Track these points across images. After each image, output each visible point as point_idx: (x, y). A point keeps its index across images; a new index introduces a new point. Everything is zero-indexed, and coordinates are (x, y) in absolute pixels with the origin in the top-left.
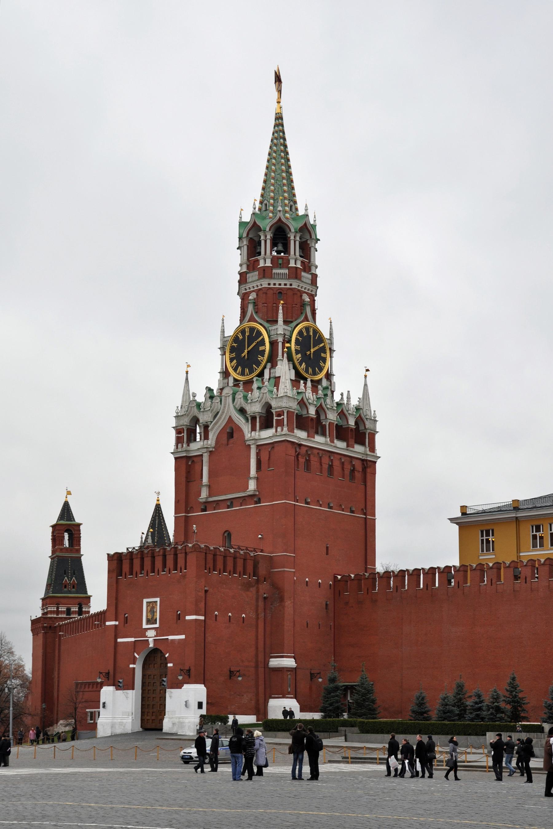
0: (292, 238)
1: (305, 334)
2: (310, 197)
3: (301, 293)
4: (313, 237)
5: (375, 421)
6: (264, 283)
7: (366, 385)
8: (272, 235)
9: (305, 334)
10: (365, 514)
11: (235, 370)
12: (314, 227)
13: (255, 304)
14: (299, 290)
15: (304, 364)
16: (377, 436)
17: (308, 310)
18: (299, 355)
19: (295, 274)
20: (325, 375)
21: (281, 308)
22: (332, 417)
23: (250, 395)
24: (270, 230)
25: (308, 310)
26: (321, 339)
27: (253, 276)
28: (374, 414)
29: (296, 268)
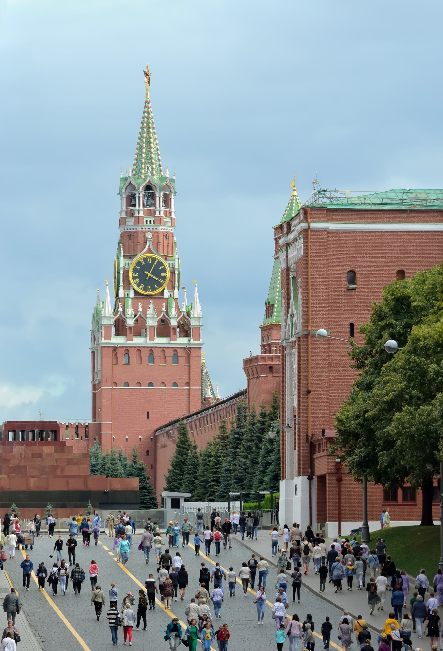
3: (144, 233)
10: (189, 386)
14: (143, 232)
15: (142, 284)
18: (138, 279)
19: (138, 220)
24: (125, 191)
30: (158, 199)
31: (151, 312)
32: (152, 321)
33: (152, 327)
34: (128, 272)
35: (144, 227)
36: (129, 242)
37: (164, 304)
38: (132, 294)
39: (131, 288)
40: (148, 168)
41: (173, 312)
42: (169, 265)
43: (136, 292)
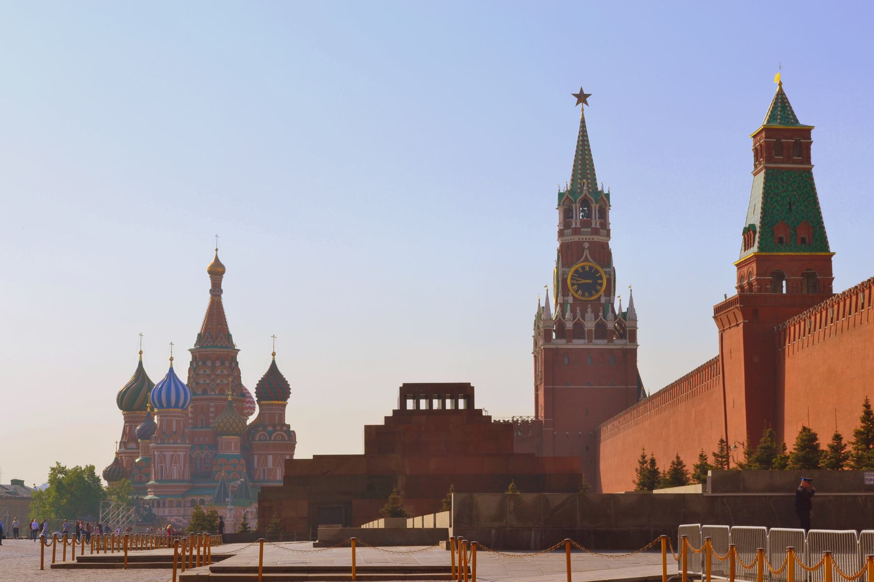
5: (636, 320)
7: (631, 297)
17: (586, 253)
22: (590, 324)
25: (586, 253)
26: (597, 271)
31: (589, 315)
32: (590, 324)
33: (590, 331)
34: (566, 279)
36: (567, 254)
37: (601, 308)
38: (570, 300)
41: (610, 315)
42: (605, 272)
43: (574, 298)
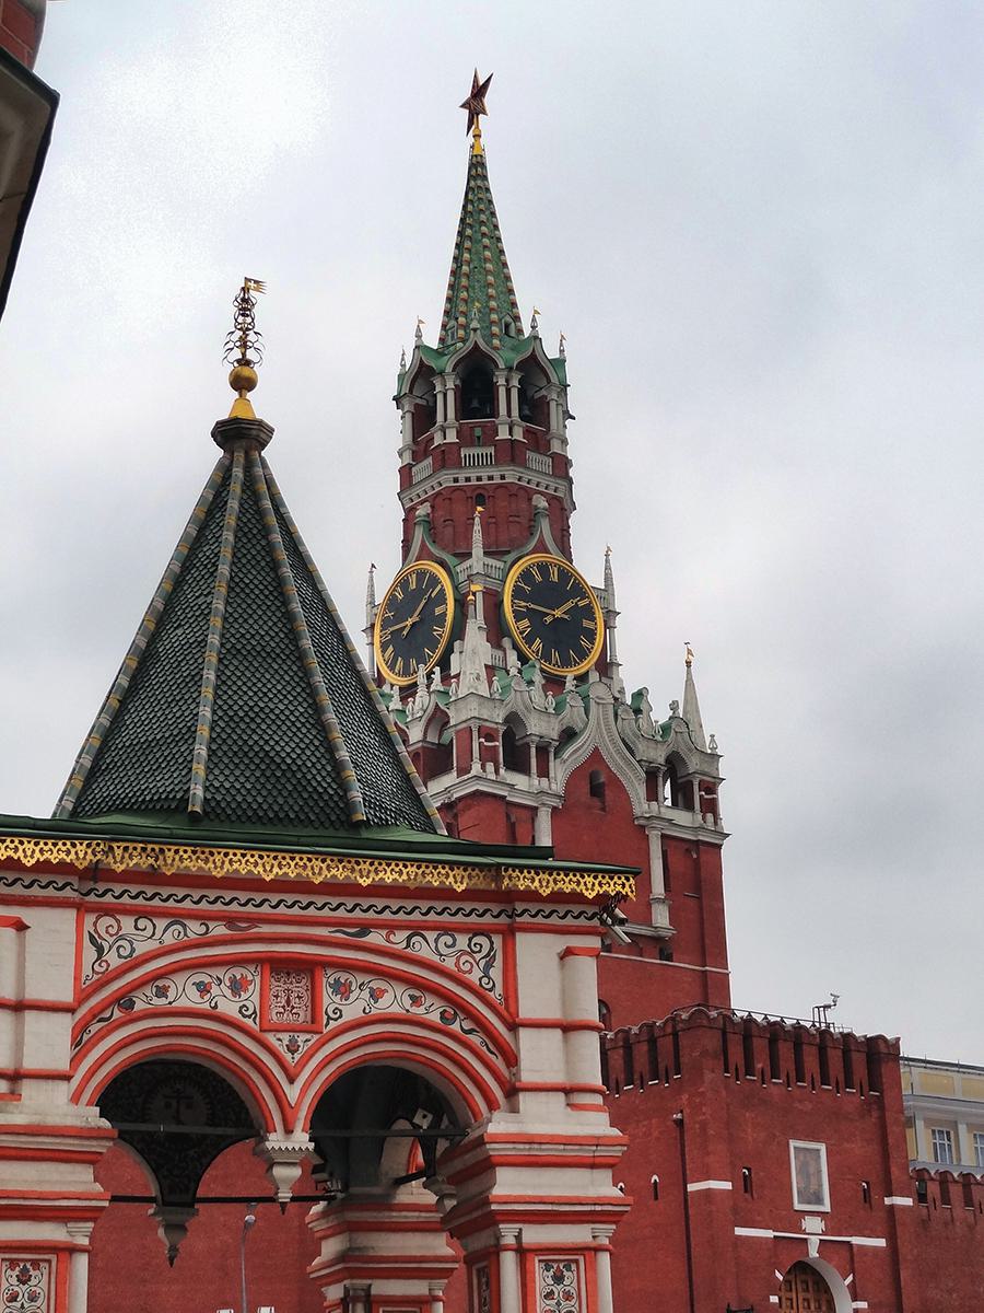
0: (502, 381)
1: (539, 578)
2: (547, 303)
3: (529, 494)
4: (554, 379)
5: (715, 757)
6: (446, 479)
7: (689, 683)
8: (458, 382)
9: (539, 578)
11: (392, 668)
12: (559, 363)
13: (430, 525)
16: (721, 789)
17: (545, 526)
18: (526, 622)
20: (596, 664)
21: (477, 520)
23: (411, 704)
25: (545, 526)
26: (579, 589)
27: (423, 468)
28: (713, 740)
29: (512, 442)
30: (553, 404)
35: (526, 477)
39: (506, 642)
40: (507, 326)
